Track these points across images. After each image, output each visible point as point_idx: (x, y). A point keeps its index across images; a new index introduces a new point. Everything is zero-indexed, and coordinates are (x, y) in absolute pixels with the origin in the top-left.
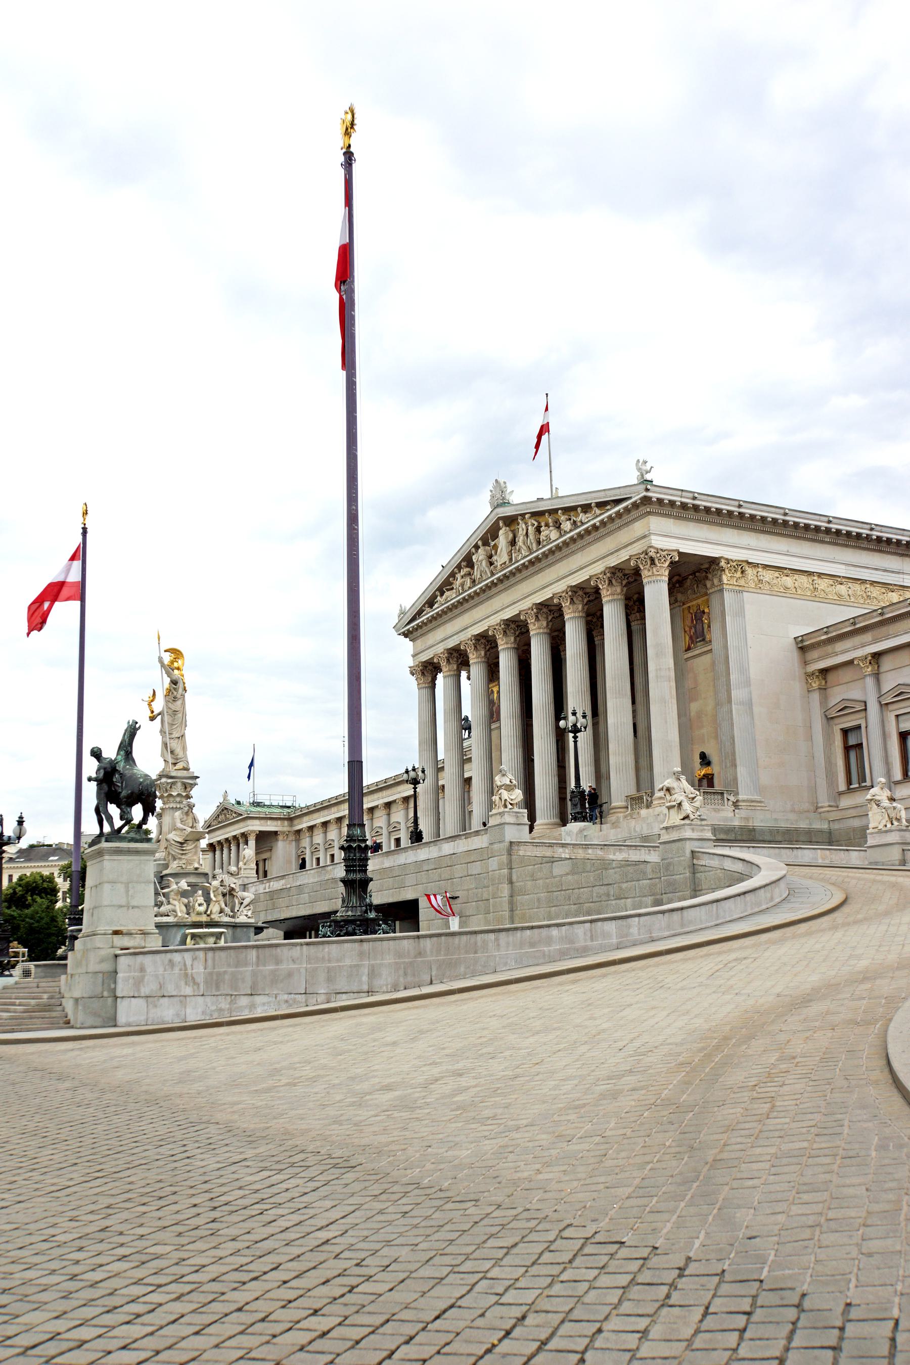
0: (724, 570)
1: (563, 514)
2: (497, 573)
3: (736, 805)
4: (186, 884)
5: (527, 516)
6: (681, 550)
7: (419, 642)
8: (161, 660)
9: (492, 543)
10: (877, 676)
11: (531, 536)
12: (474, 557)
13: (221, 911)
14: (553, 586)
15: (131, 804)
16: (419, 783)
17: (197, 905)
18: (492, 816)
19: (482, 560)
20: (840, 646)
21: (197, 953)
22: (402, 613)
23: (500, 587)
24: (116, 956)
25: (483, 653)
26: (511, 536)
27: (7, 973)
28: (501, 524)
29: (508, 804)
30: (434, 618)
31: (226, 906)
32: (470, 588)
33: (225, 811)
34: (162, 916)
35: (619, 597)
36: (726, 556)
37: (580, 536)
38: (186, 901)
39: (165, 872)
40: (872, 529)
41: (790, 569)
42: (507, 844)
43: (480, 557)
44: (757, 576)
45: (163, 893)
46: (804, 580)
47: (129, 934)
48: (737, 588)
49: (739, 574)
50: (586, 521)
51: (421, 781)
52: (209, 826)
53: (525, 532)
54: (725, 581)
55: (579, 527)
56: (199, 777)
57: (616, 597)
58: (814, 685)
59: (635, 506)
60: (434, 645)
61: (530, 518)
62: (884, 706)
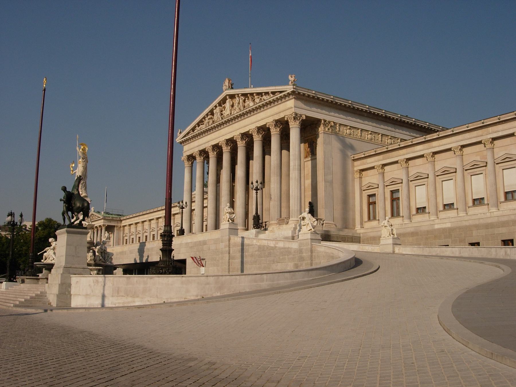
1: (256, 95)
2: (225, 119)
5: (240, 95)
6: (307, 115)
11: (241, 104)
12: (214, 111)
14: (249, 126)
15: (78, 213)
16: (184, 208)
19: (218, 113)
20: (369, 160)
26: (231, 103)
27: (15, 280)
28: (228, 97)
29: (230, 220)
30: (194, 137)
32: (212, 124)
37: (263, 106)
41: (350, 126)
43: (217, 111)
50: (266, 99)
51: (185, 208)
53: (238, 102)
55: (262, 102)
57: (277, 133)
59: (288, 93)
61: (241, 96)
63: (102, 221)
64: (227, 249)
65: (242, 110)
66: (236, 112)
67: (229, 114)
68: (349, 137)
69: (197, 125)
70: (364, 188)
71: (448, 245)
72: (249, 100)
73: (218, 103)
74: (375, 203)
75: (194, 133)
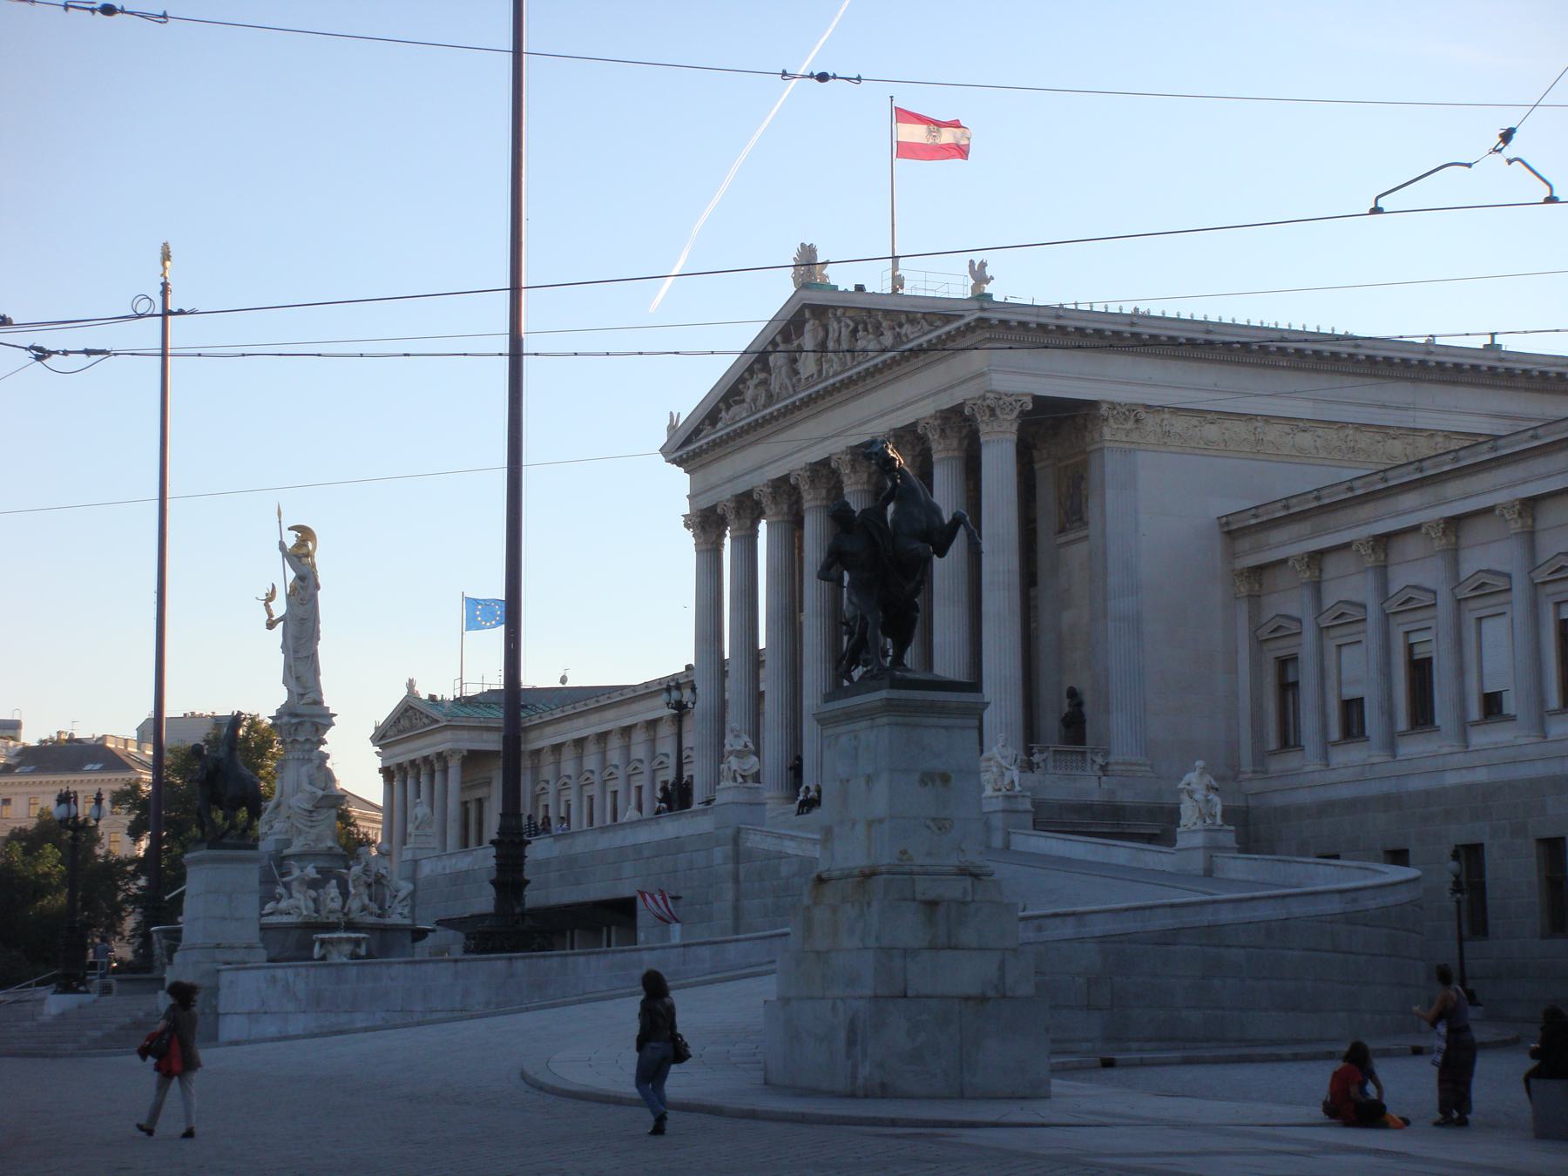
0: (1107, 420)
1: (885, 318)
3: (1104, 768)
4: (314, 870)
7: (699, 474)
8: (282, 546)
9: (796, 343)
10: (1317, 587)
12: (771, 358)
13: (364, 908)
15: (236, 808)
17: (328, 901)
18: (718, 790)
19: (781, 367)
20: (1277, 536)
21: (299, 970)
22: (672, 428)
23: (806, 412)
24: (218, 971)
25: (785, 508)
26: (821, 334)
27: (81, 988)
28: (807, 314)
29: (738, 776)
30: (715, 445)
31: (370, 900)
33: (411, 712)
34: (281, 914)
35: (956, 453)
36: (1110, 399)
38: (313, 893)
39: (287, 852)
40: (1357, 346)
42: (730, 832)
44: (1161, 426)
45: (283, 882)
46: (1241, 428)
47: (231, 948)
48: (1127, 446)
49: (1130, 425)
51: (690, 705)
52: (381, 739)
53: (836, 335)
54: (1108, 437)
56: (335, 715)
58: (1242, 589)
59: (969, 328)
60: (719, 486)
62: (1322, 631)
63: (448, 734)
64: (730, 866)
65: (849, 365)
66: (836, 369)
67: (815, 376)
68: (1212, 453)
69: (722, 405)
70: (1264, 633)
71: (1337, 857)
72: (868, 333)
73: (779, 333)
74: (1296, 684)
75: (716, 432)
